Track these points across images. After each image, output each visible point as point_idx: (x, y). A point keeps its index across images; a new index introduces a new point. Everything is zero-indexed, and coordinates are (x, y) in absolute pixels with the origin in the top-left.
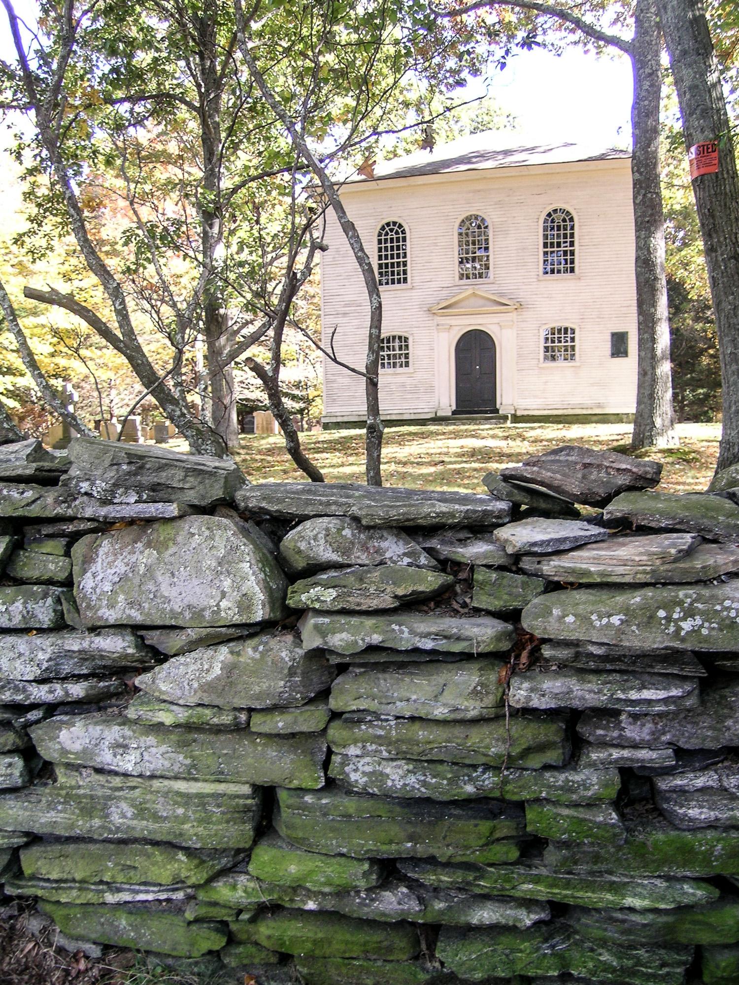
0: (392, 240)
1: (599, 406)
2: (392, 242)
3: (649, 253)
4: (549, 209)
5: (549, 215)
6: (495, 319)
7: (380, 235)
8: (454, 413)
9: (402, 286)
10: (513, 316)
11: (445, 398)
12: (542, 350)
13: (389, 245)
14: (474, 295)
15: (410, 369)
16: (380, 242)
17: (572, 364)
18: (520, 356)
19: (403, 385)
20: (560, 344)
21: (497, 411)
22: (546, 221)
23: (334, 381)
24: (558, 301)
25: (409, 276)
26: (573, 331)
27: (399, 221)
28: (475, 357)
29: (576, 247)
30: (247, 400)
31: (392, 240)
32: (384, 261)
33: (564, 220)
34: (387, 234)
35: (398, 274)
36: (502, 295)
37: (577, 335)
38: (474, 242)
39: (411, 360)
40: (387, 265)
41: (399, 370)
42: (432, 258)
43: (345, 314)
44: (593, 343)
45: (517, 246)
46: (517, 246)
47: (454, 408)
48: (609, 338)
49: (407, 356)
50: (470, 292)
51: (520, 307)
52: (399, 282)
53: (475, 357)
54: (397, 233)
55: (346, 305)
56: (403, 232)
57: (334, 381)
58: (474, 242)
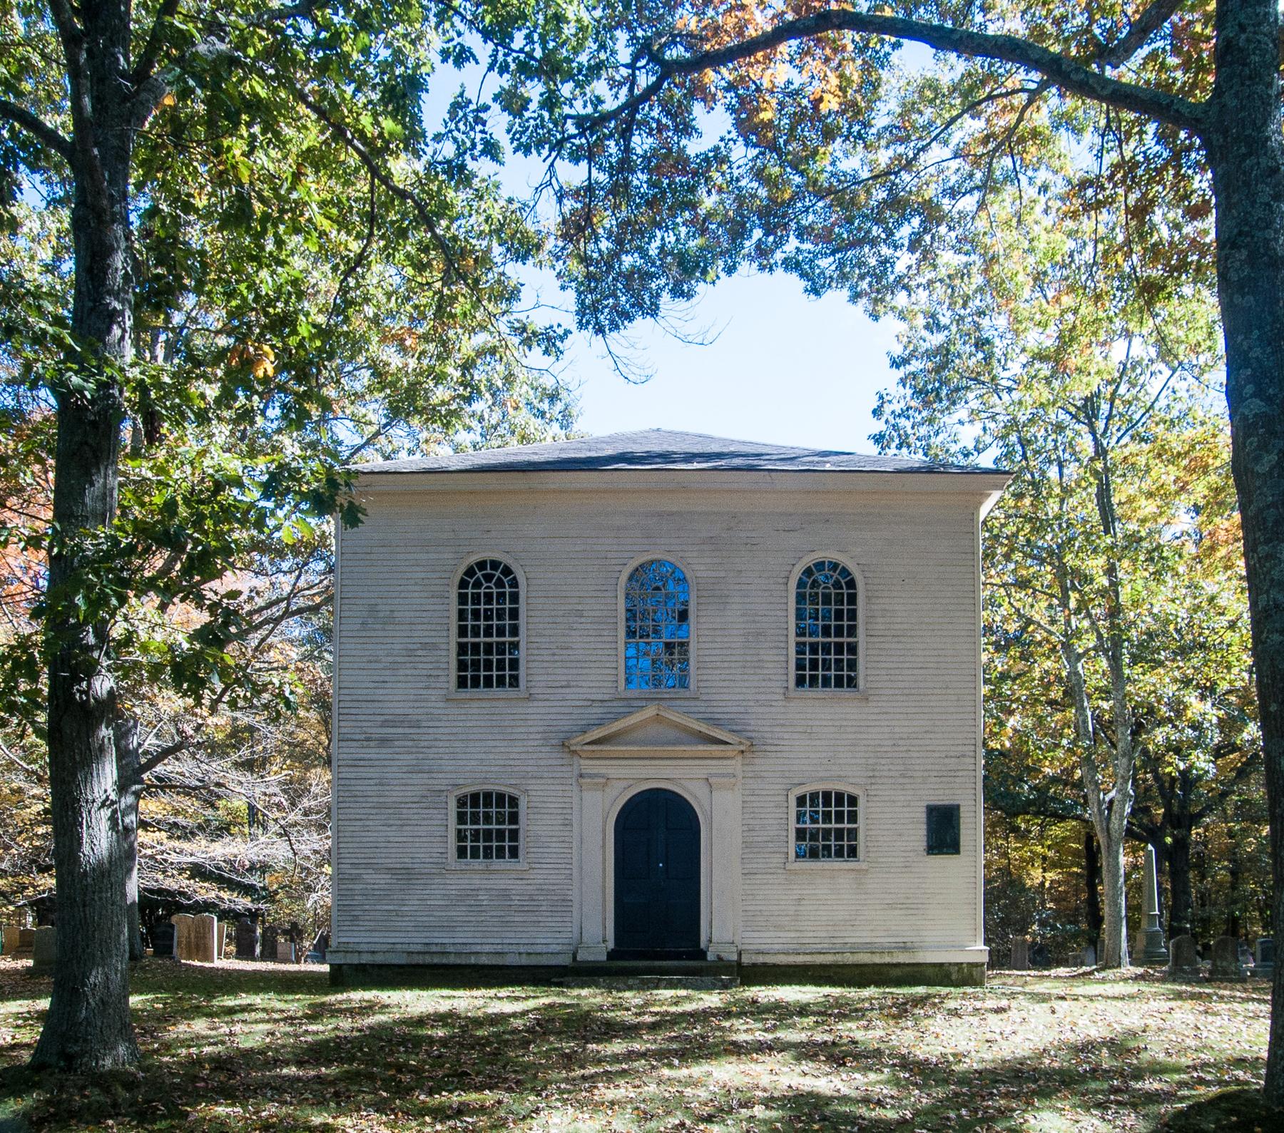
0: (489, 597)
1: (905, 948)
2: (489, 601)
3: (1231, 981)
4: (809, 560)
5: (808, 572)
6: (699, 770)
7: (463, 584)
8: (611, 955)
9: (508, 692)
10: (736, 765)
11: (594, 924)
12: (792, 835)
13: (495, 658)
14: (658, 718)
15: (522, 864)
16: (462, 599)
17: (851, 865)
18: (747, 845)
19: (505, 895)
20: (828, 827)
21: (702, 955)
22: (801, 584)
23: (355, 879)
24: (819, 740)
25: (522, 672)
26: (853, 801)
27: (506, 559)
28: (658, 842)
29: (861, 638)
30: (160, 891)
31: (489, 597)
32: (470, 639)
33: (837, 585)
34: (477, 584)
35: (488, 618)
36: (716, 722)
37: (861, 809)
38: (657, 616)
39: (522, 843)
40: (476, 647)
41: (496, 864)
42: (574, 647)
43: (384, 741)
44: (891, 824)
45: (744, 641)
46: (744, 641)
47: (611, 945)
48: (922, 816)
49: (514, 835)
50: (650, 711)
51: (751, 748)
52: (501, 682)
53: (658, 842)
54: (500, 584)
55: (384, 724)
56: (514, 583)
57: (355, 879)
58: (657, 616)
